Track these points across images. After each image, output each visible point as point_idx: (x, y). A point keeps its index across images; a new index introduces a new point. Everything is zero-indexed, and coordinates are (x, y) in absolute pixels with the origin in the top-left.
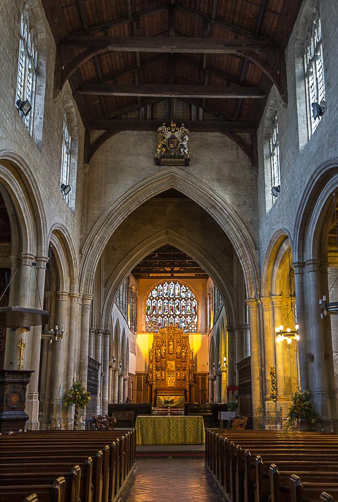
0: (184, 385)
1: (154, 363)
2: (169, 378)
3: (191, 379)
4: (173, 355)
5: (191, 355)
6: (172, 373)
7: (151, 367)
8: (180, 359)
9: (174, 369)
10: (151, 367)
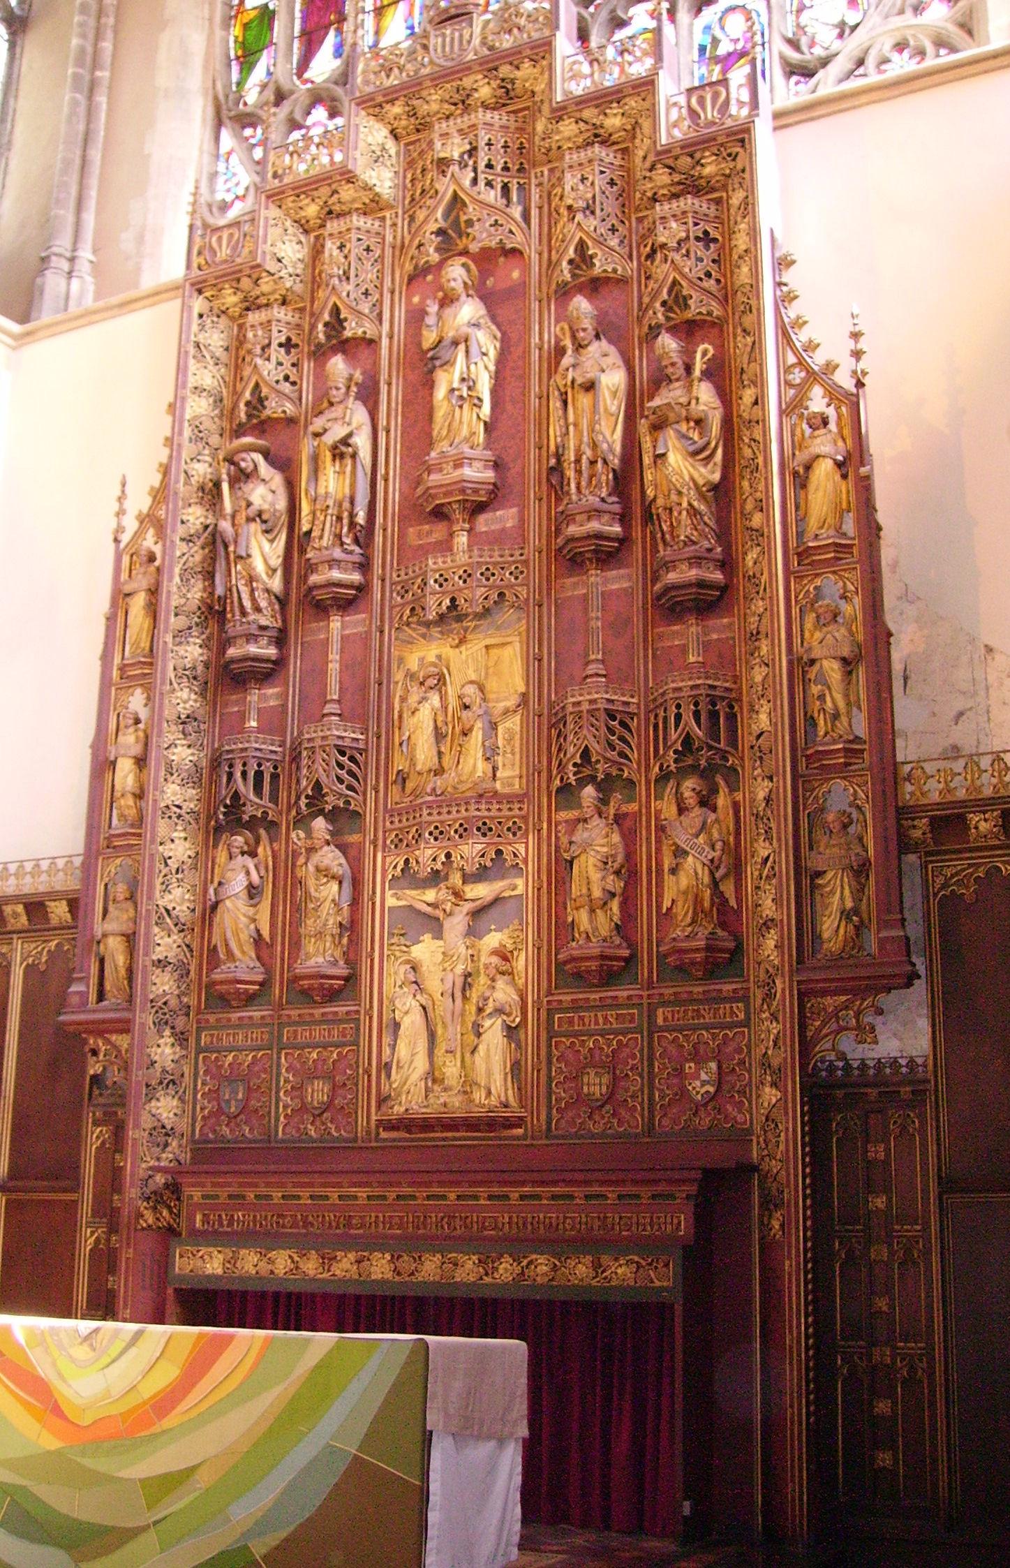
0: (701, 1083)
1: (185, 699)
2: (425, 950)
3: (831, 927)
4: (503, 518)
5: (826, 445)
6: (471, 850)
7: (125, 774)
8: (618, 580)
9: (510, 775)
10: (125, 774)
